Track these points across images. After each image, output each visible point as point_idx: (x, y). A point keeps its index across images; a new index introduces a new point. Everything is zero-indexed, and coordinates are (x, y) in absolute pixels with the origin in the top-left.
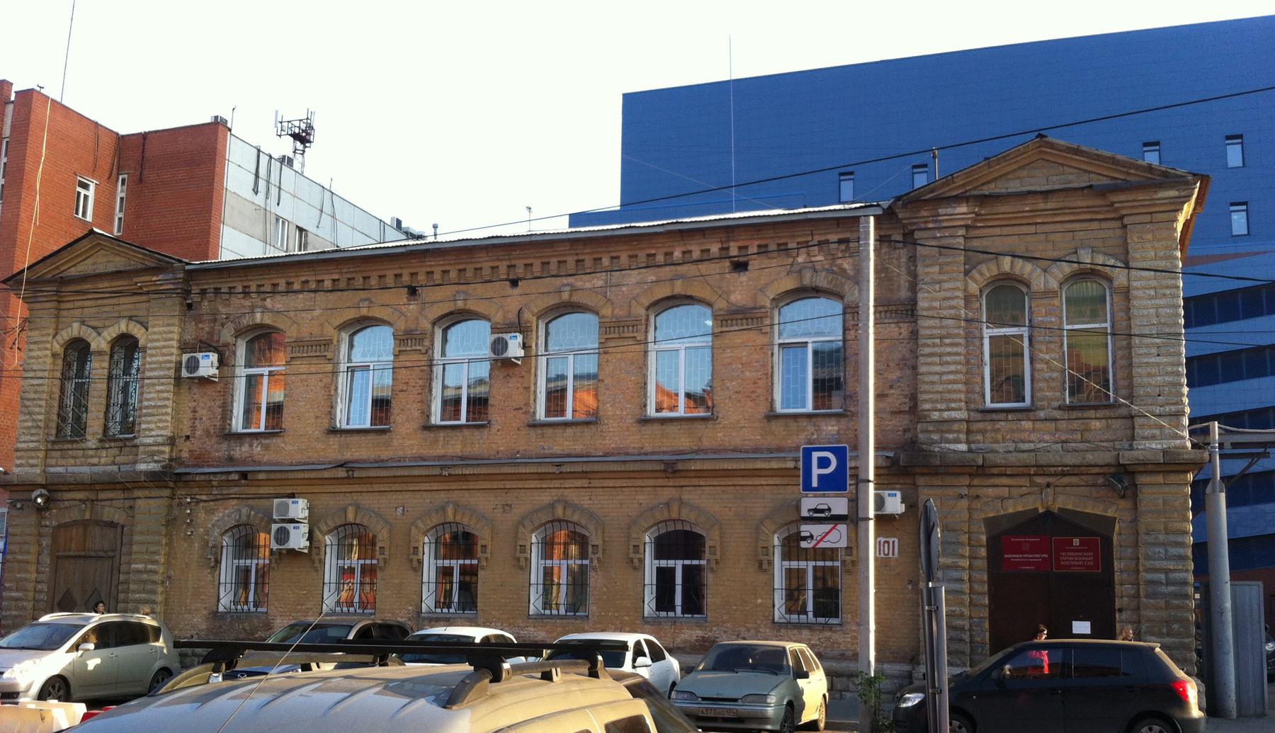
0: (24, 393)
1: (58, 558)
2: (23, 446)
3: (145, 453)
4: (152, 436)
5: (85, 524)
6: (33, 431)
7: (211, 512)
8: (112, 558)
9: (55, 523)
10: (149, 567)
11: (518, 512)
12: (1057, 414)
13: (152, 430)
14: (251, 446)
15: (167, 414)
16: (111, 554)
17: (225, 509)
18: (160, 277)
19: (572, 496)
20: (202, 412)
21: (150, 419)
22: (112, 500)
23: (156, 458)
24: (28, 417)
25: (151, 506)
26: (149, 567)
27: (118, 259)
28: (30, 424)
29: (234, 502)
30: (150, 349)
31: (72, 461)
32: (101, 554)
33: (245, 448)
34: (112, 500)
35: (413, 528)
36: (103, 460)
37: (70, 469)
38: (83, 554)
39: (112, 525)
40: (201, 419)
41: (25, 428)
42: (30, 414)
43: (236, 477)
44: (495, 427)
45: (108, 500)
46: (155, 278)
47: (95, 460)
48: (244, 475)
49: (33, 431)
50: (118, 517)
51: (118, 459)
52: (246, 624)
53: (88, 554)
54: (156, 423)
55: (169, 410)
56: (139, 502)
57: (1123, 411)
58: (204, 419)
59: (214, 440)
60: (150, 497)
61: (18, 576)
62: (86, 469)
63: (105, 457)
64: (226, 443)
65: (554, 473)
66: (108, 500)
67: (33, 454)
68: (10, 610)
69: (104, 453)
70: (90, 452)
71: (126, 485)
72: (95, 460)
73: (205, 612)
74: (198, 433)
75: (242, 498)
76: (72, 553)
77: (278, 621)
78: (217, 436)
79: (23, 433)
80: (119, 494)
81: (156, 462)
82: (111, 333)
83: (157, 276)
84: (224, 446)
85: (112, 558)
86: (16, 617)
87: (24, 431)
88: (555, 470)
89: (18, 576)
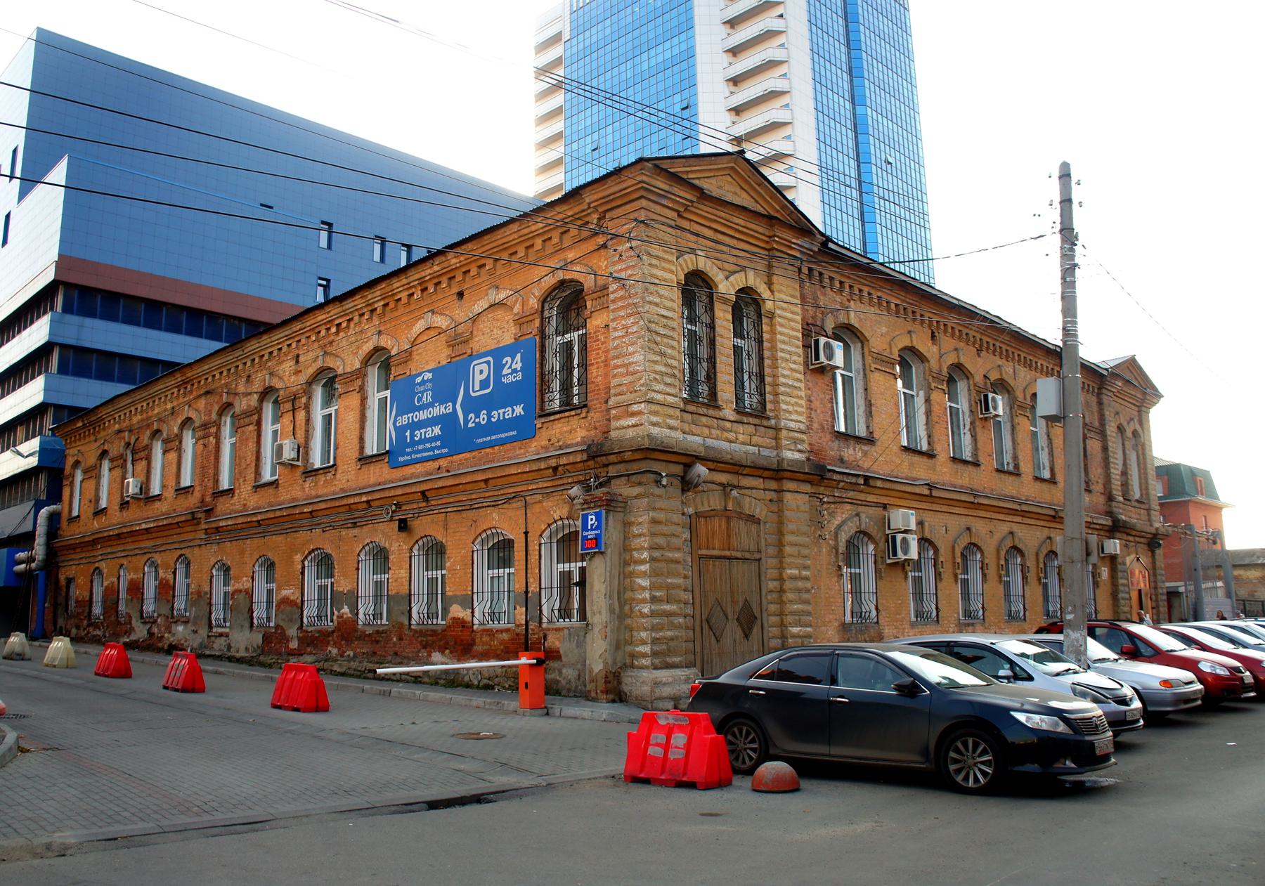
0: (650, 322)
1: (701, 557)
2: (659, 397)
3: (789, 438)
4: (792, 420)
5: (726, 514)
6: (668, 380)
7: (832, 514)
8: (759, 560)
9: (691, 511)
10: (804, 573)
11: (998, 536)
12: (1136, 504)
13: (790, 412)
14: (855, 450)
15: (801, 398)
16: (757, 556)
17: (843, 513)
18: (799, 242)
19: (1015, 528)
20: (816, 404)
21: (788, 399)
22: (752, 488)
23: (799, 447)
24: (658, 358)
25: (797, 500)
26: (804, 573)
27: (744, 195)
28: (661, 368)
29: (848, 507)
30: (780, 317)
31: (706, 431)
32: (747, 555)
33: (851, 451)
34: (752, 488)
35: (956, 545)
36: (741, 437)
37: (710, 442)
38: (727, 553)
39: (752, 519)
40: (816, 411)
41: (656, 372)
42: (662, 354)
43: (861, 481)
44: (983, 467)
45: (748, 488)
46: (794, 241)
47: (732, 436)
48: (867, 478)
49: (668, 380)
50: (760, 510)
51: (755, 439)
52: (866, 635)
53: (734, 554)
54: (793, 405)
55: (803, 394)
56: (788, 496)
57: (1147, 507)
58: (818, 411)
59: (828, 437)
60: (797, 492)
61: (669, 581)
62: (725, 445)
63: (743, 432)
64: (837, 442)
65: (1017, 510)
66: (748, 488)
67: (671, 411)
68: (661, 630)
69: (741, 428)
70: (728, 425)
71: (777, 473)
72: (732, 436)
73: (836, 624)
74: (816, 426)
75: (854, 504)
76: (716, 553)
77: (887, 631)
78: (830, 433)
79: (655, 379)
80: (757, 482)
81: (800, 451)
82: (739, 281)
83: (798, 238)
84: (836, 444)
85: (759, 560)
86: (672, 639)
87: (657, 377)
88: (1018, 507)
89: (669, 581)
